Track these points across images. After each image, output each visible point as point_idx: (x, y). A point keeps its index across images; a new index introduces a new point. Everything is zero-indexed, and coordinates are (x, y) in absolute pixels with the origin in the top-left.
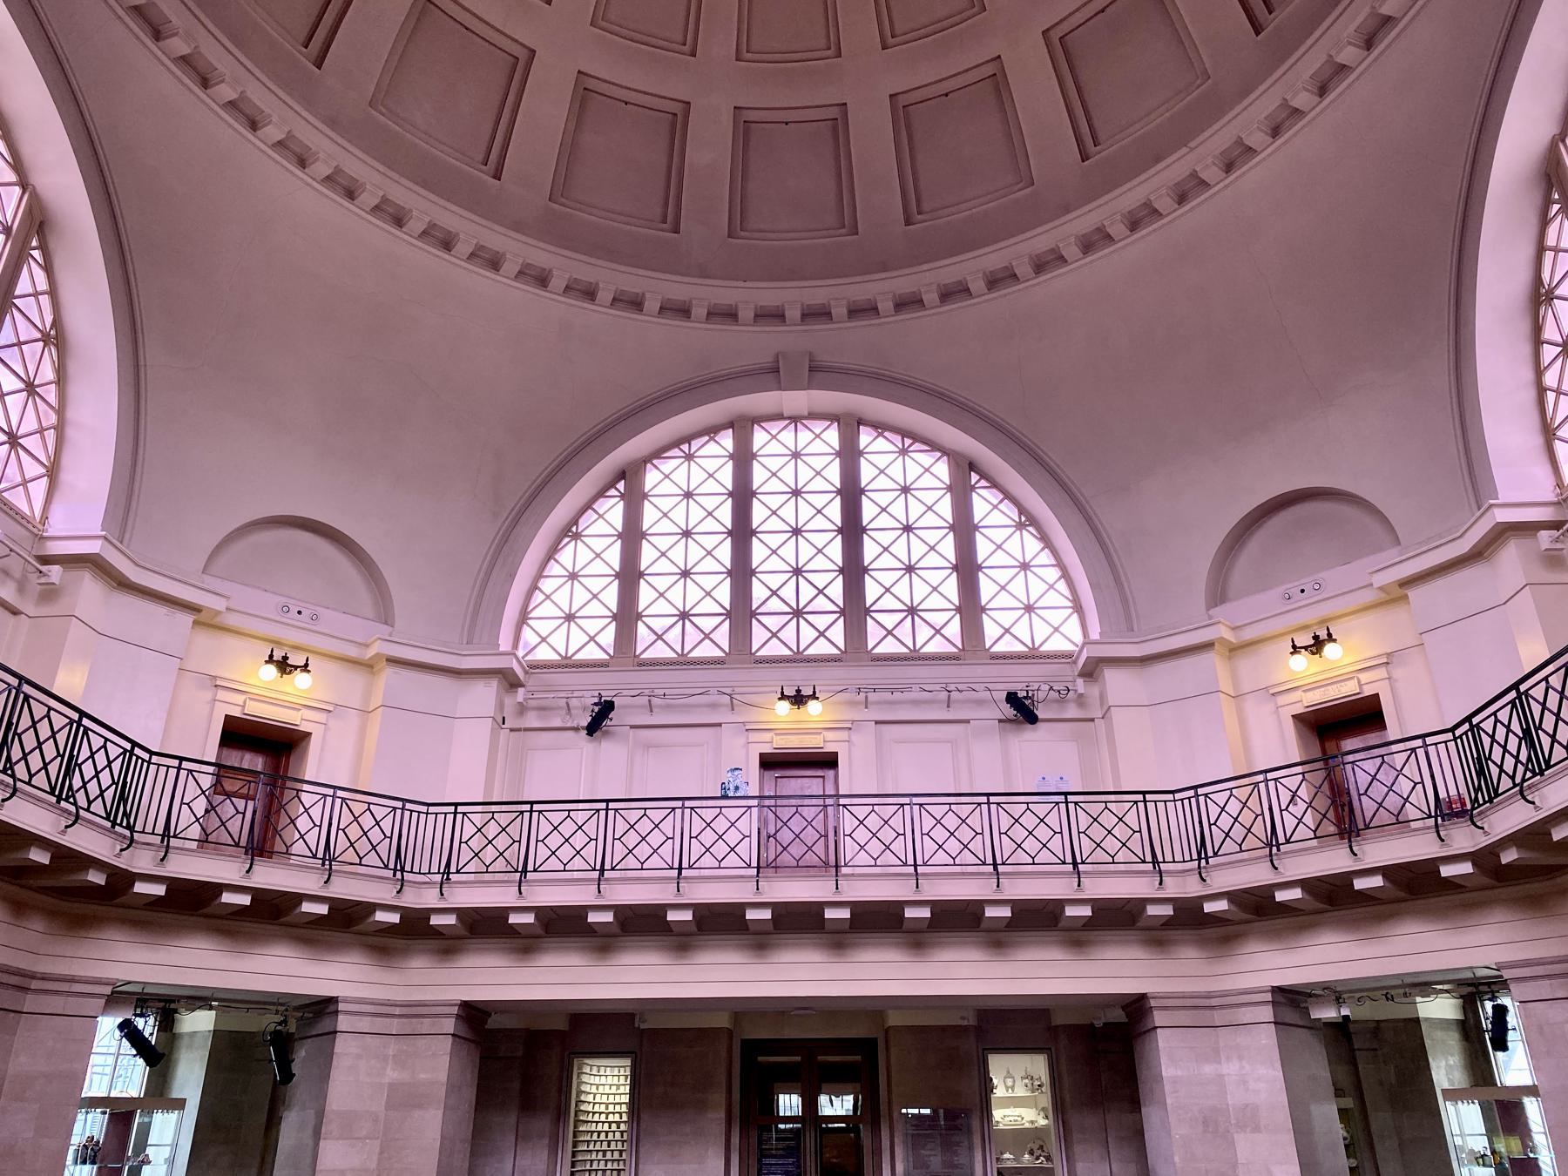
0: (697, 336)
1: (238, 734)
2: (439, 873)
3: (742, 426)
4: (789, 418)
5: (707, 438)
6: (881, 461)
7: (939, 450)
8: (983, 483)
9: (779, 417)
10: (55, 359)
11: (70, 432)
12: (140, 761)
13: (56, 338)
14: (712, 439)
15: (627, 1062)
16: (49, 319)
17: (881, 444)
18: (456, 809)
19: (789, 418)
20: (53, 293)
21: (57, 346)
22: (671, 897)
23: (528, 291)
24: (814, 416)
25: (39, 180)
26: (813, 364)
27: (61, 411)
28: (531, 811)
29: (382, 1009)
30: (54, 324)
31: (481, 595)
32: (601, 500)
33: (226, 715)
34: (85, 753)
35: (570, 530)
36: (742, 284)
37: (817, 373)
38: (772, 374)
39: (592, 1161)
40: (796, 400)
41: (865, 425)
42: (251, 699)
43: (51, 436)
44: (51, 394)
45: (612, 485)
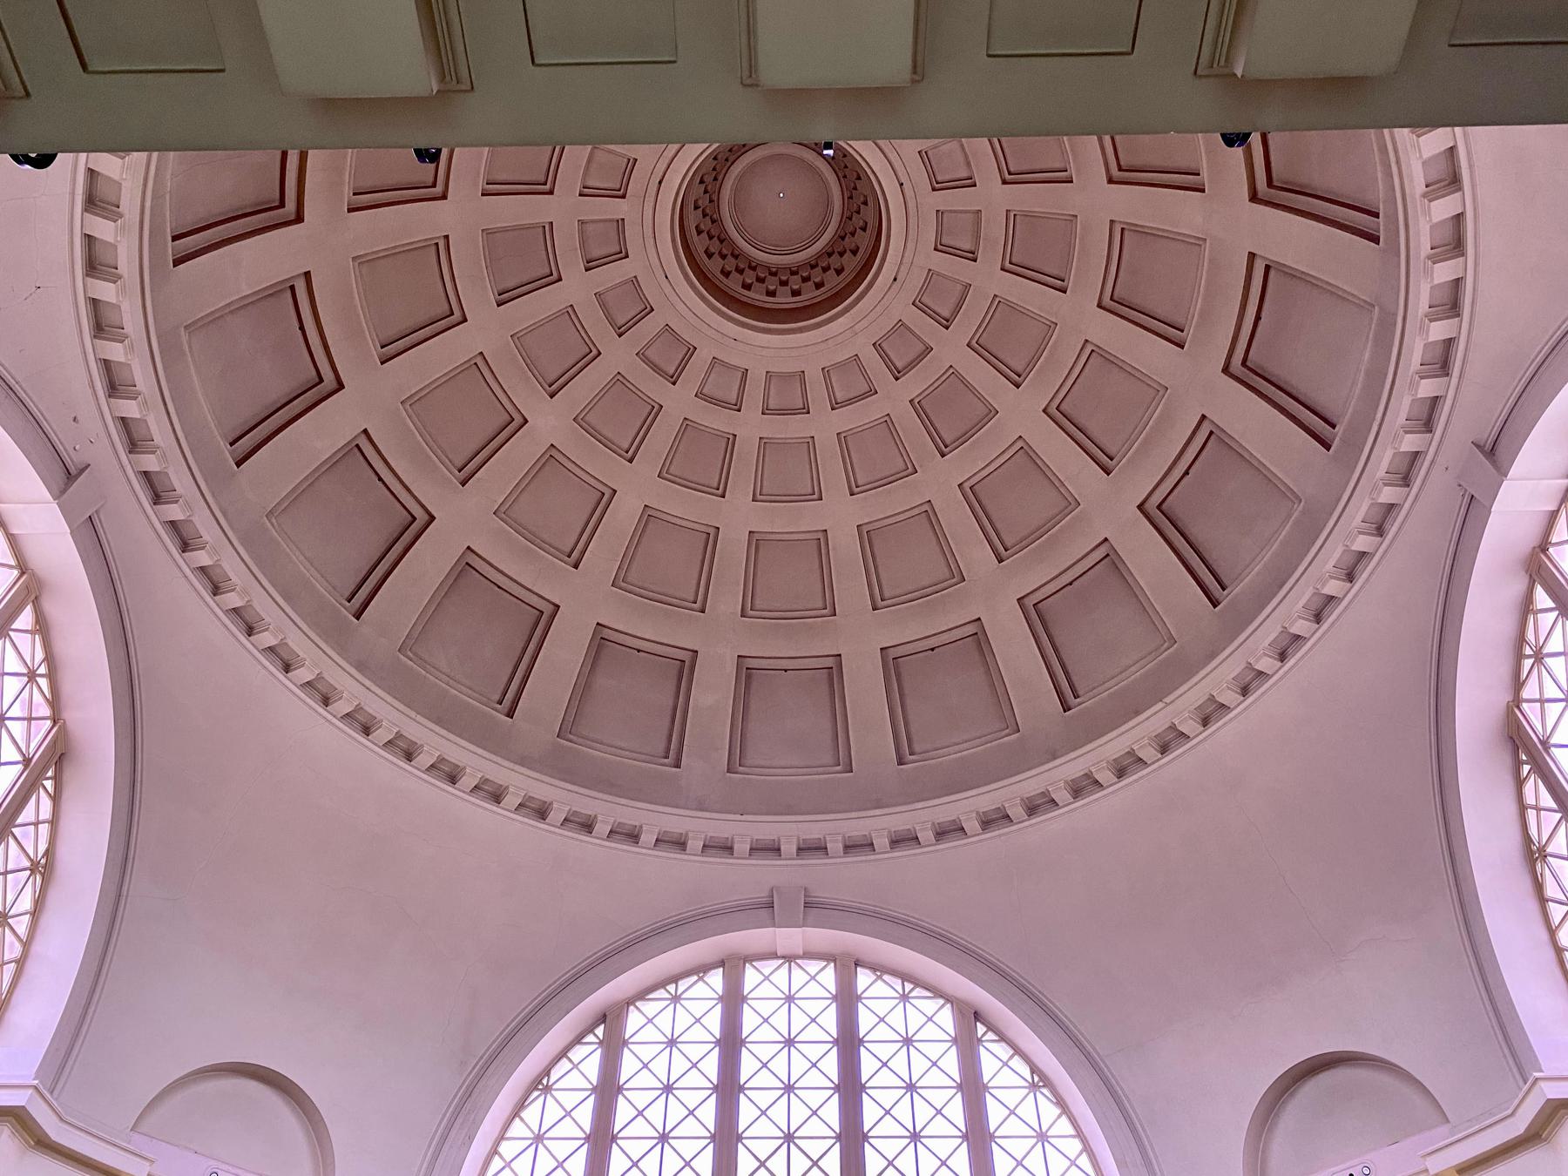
0: (691, 869)
3: (733, 965)
4: (783, 957)
5: (695, 978)
6: (881, 1007)
7: (941, 997)
8: (991, 1036)
9: (773, 955)
10: (37, 893)
11: (31, 967)
13: (45, 867)
14: (701, 979)
16: (42, 848)
17: (880, 989)
20: (54, 822)
21: (43, 875)
23: (527, 822)
24: (809, 955)
25: (71, 716)
26: (809, 899)
27: (27, 945)
30: (47, 853)
31: (436, 1157)
32: (578, 1047)
35: (540, 1082)
36: (738, 817)
37: (813, 908)
38: (766, 909)
40: (789, 937)
41: (861, 966)
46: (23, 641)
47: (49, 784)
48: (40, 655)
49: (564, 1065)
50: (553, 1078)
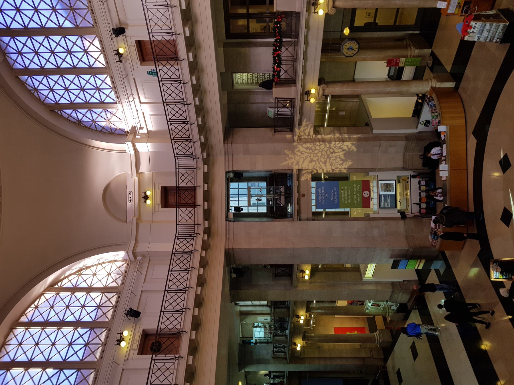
1: (166, 204)
2: (193, 160)
12: (179, 234)
14: (25, 83)
15: (234, 74)
18: (160, 81)
19: (4, 56)
28: (162, 81)
34: (180, 250)
39: (260, 78)
43: (104, 265)
44: (93, 269)
45: (57, 113)
46: (29, 315)
47: (59, 284)
48: (30, 309)
49: (70, 118)
50: (76, 121)
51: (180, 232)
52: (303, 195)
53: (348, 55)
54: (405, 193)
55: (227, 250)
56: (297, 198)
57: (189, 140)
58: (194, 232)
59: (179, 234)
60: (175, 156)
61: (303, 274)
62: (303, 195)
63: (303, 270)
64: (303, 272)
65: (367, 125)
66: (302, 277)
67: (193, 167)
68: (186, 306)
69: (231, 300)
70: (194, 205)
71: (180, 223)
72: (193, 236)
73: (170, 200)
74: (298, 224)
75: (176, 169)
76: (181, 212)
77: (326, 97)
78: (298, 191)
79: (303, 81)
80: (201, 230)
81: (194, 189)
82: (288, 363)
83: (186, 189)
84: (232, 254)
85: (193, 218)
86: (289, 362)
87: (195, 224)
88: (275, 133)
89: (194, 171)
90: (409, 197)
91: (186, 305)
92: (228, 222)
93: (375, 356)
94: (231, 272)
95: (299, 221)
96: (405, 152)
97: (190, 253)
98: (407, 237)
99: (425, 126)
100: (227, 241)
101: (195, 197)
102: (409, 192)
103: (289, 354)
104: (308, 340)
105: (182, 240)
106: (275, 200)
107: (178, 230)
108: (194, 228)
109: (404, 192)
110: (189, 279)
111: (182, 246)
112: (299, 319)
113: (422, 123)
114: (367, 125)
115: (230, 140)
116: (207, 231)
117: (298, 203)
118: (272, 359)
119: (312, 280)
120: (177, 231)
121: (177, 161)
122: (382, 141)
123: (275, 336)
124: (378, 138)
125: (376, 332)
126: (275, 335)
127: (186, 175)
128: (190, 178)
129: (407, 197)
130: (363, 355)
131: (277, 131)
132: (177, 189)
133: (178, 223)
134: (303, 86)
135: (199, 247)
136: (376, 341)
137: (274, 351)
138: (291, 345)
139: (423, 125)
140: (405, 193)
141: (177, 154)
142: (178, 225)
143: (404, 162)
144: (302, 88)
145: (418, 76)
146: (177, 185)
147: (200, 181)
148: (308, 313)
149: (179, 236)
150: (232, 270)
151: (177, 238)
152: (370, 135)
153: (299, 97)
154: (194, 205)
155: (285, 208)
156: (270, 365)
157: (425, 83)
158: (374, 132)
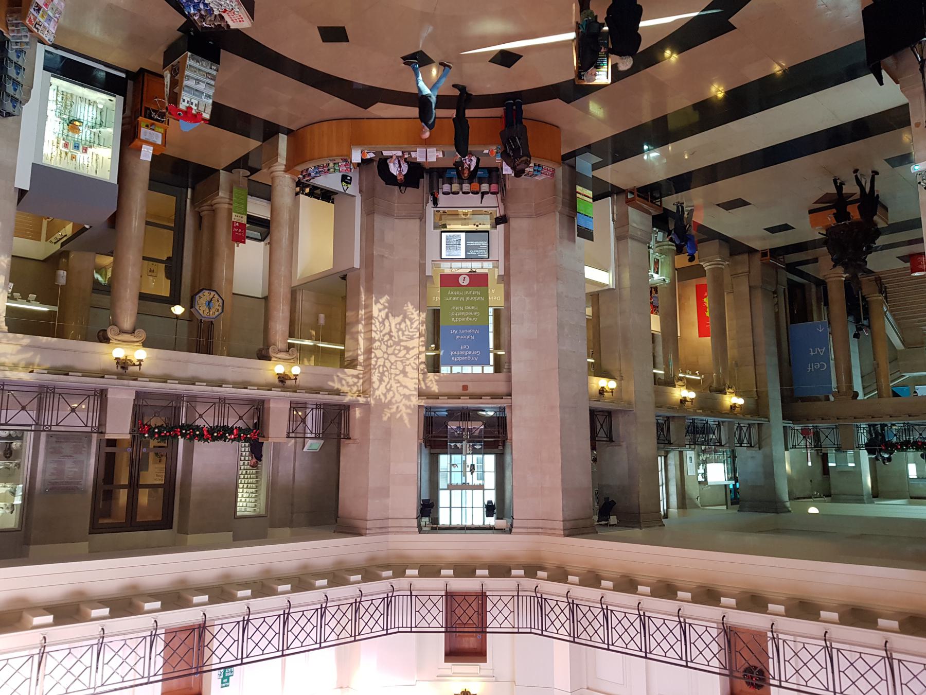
1: (479, 654)
2: (395, 596)
12: (536, 627)
15: (239, 514)
22: (107, 624)
29: (399, 530)
33: (486, 662)
42: (477, 674)
51: (533, 627)
52: (465, 388)
53: (220, 309)
54: (464, 217)
55: (567, 532)
56: (470, 398)
57: (356, 605)
58: (532, 598)
59: (536, 627)
60: (387, 634)
61: (607, 392)
62: (465, 388)
63: (600, 390)
64: (603, 390)
65: (344, 278)
66: (612, 392)
67: (409, 597)
68: (675, 616)
69: (660, 526)
70: (482, 596)
71: (516, 626)
72: (540, 599)
73: (471, 646)
74: (516, 399)
75: (411, 632)
76: (495, 624)
77: (291, 346)
78: (458, 397)
79: (260, 386)
80: (529, 583)
81: (450, 596)
82: (769, 421)
83: (449, 612)
84: (573, 522)
85: (506, 599)
86: (767, 420)
87: (518, 596)
88: (350, 439)
89: (416, 596)
90: (471, 210)
91: (673, 615)
92: (513, 530)
93: (747, 269)
94: (607, 525)
95: (511, 396)
96: (394, 216)
97: (573, 606)
98: (539, 215)
99: (350, 184)
100: (549, 531)
101: (465, 595)
102: (460, 210)
103: (751, 418)
104: (725, 385)
105: (548, 623)
106: (473, 440)
107: (529, 630)
108: (524, 598)
109: (462, 219)
110: (622, 610)
111: (560, 623)
112: (688, 399)
113: (345, 188)
114: (344, 278)
115: (359, 523)
116: (531, 571)
117: (480, 397)
118: (762, 450)
119: (617, 375)
120: (531, 633)
121: (396, 630)
122: (373, 254)
123: (721, 443)
124: (368, 260)
125: (704, 266)
126: (719, 444)
127: (424, 611)
128: (429, 605)
129: (469, 213)
130: (745, 289)
131: (348, 435)
132: (449, 630)
133: (516, 630)
134: (269, 387)
135: (561, 588)
136: (720, 266)
137: (749, 445)
138: (736, 415)
139: (348, 185)
140: (464, 217)
141: (383, 630)
142: (521, 630)
143: (410, 217)
144: (273, 389)
145: (265, 193)
146: (443, 630)
147: (435, 585)
148: (676, 383)
149: (540, 628)
150: (603, 523)
151: (545, 633)
152: (363, 273)
153: (288, 394)
154: (482, 596)
155: (488, 421)
156: (774, 454)
157: (277, 181)
158: (357, 265)
